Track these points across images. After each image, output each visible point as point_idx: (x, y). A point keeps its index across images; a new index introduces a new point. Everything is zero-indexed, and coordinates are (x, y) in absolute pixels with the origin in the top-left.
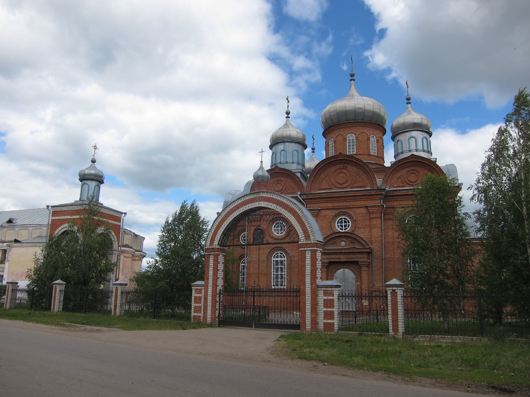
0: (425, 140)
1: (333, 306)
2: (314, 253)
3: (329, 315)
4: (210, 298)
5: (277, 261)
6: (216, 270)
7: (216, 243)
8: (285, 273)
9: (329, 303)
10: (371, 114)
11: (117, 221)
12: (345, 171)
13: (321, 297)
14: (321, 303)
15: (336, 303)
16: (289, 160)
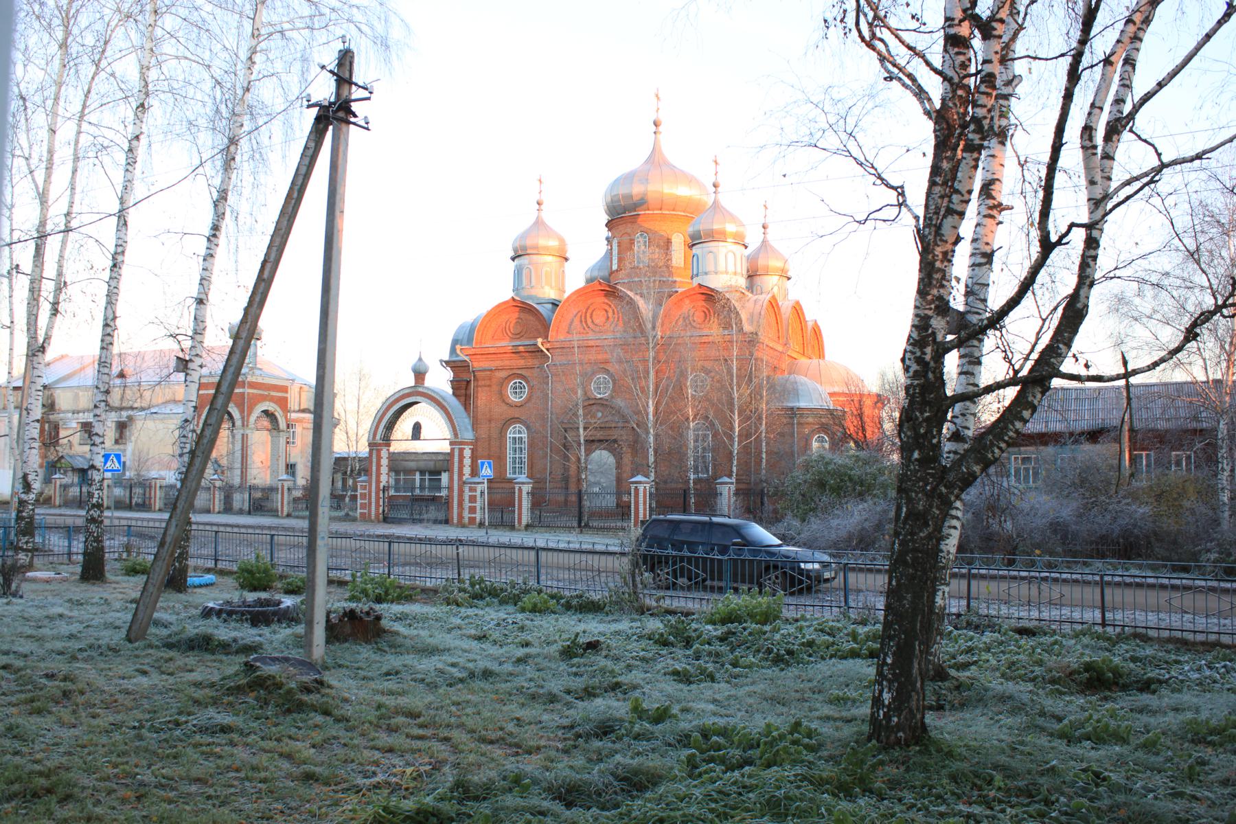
0: (730, 256)
1: (475, 502)
2: (461, 450)
3: (472, 510)
4: (373, 495)
5: (514, 438)
7: (378, 437)
8: (525, 455)
9: (473, 499)
11: (282, 392)
14: (467, 499)
15: (478, 498)
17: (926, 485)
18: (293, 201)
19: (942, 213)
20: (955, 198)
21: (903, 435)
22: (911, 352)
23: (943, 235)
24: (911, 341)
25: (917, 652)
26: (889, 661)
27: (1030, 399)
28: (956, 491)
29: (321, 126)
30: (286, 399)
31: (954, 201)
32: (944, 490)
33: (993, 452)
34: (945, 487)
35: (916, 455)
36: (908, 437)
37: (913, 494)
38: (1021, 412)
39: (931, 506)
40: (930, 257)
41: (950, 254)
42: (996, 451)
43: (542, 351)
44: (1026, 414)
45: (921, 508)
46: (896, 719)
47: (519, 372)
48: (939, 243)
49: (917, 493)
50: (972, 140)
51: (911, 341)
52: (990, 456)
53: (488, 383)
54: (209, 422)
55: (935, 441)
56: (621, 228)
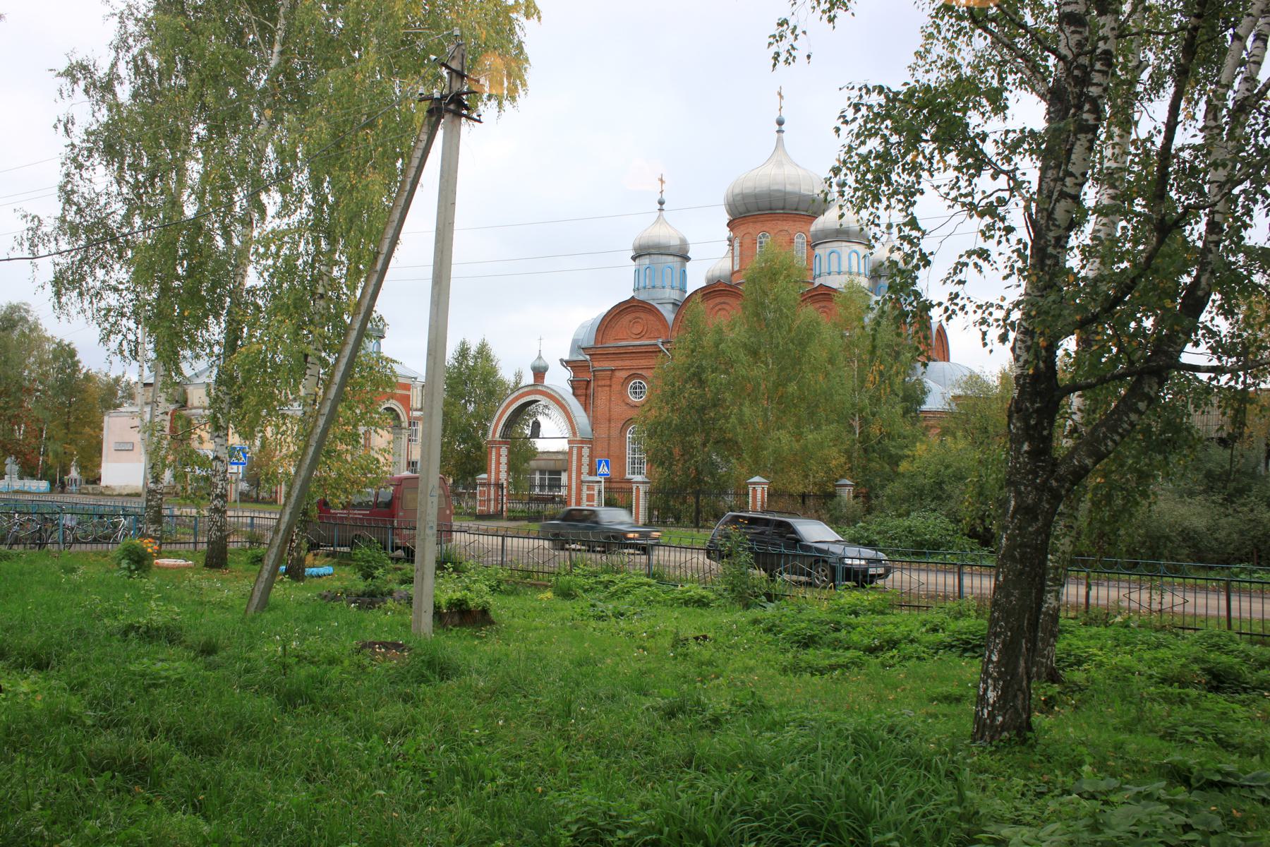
0: (854, 257)
6: (498, 463)
7: (497, 435)
10: (797, 199)
12: (724, 306)
13: (585, 492)
14: (584, 497)
16: (658, 284)
17: (1036, 478)
18: (406, 194)
19: (1054, 197)
20: (1069, 181)
21: (1012, 427)
22: (1021, 340)
23: (1055, 220)
24: (1022, 329)
25: (1024, 650)
26: (995, 658)
27: (1146, 390)
28: (1067, 485)
29: (434, 119)
30: (408, 397)
31: (1067, 184)
32: (1054, 484)
33: (1106, 445)
34: (1056, 480)
35: (1026, 447)
36: (1018, 429)
37: (1023, 488)
38: (1136, 403)
39: (1040, 500)
40: (1042, 242)
41: (1064, 240)
42: (1110, 443)
43: (660, 351)
44: (1142, 406)
45: (1030, 501)
46: (1000, 719)
47: (639, 372)
48: (1052, 228)
49: (1026, 486)
50: (1087, 120)
51: (1022, 329)
52: (1103, 448)
53: (608, 382)
54: (322, 412)
55: (1045, 433)
56: (742, 228)
